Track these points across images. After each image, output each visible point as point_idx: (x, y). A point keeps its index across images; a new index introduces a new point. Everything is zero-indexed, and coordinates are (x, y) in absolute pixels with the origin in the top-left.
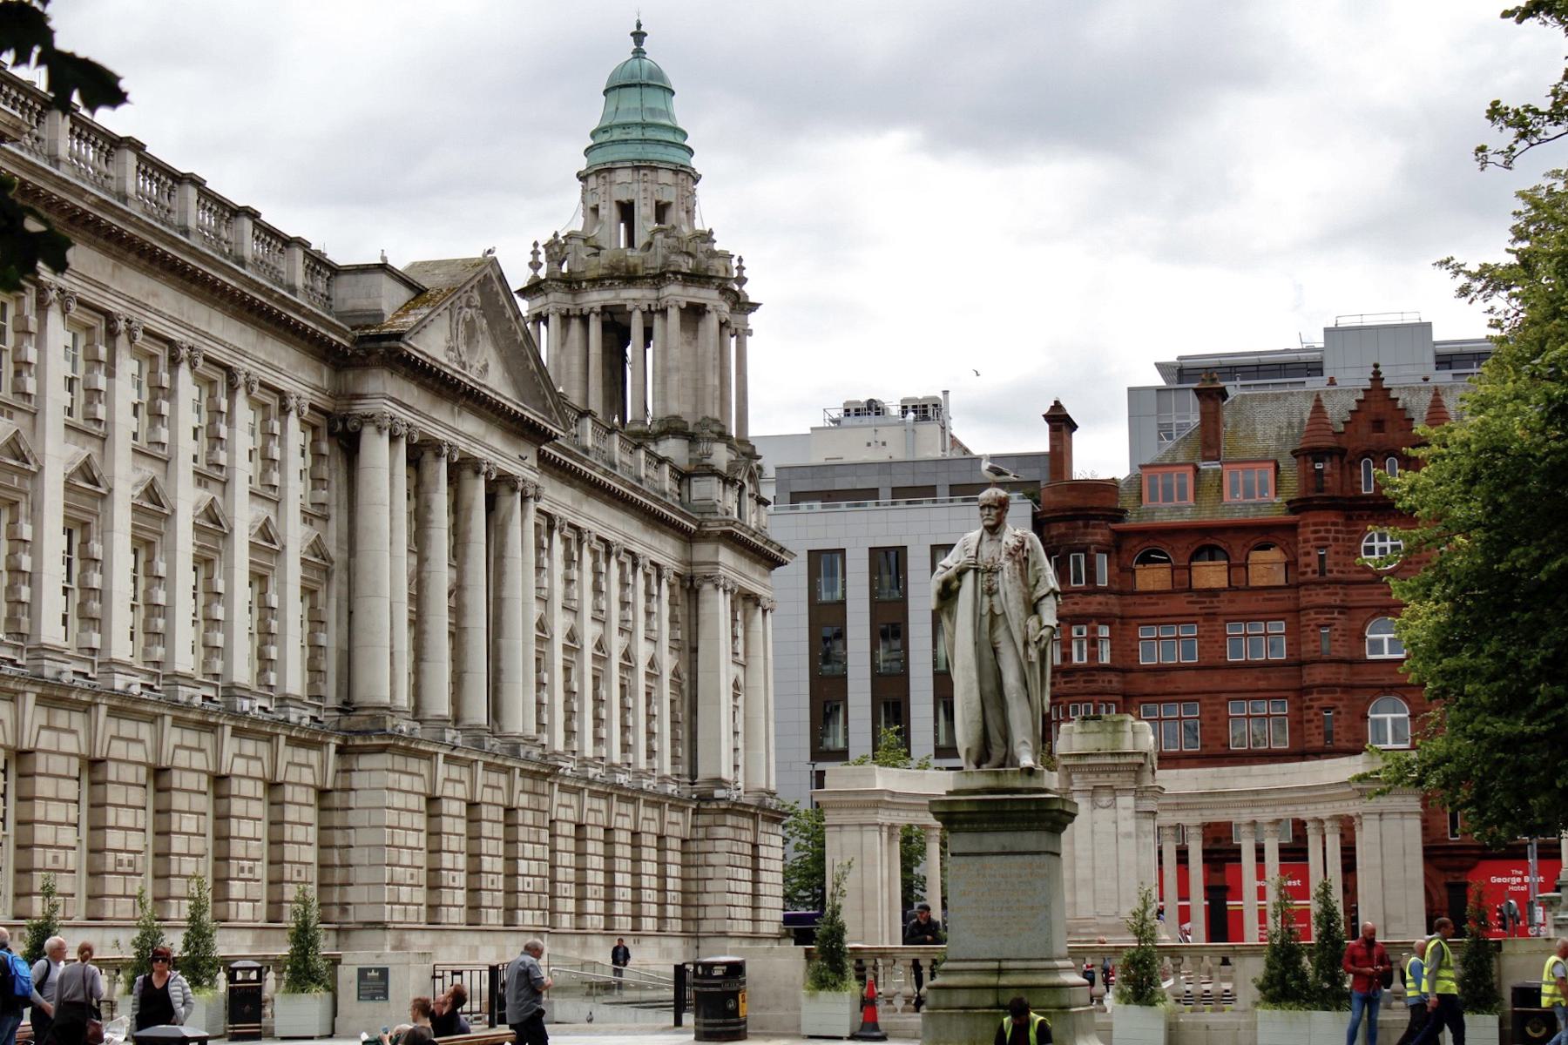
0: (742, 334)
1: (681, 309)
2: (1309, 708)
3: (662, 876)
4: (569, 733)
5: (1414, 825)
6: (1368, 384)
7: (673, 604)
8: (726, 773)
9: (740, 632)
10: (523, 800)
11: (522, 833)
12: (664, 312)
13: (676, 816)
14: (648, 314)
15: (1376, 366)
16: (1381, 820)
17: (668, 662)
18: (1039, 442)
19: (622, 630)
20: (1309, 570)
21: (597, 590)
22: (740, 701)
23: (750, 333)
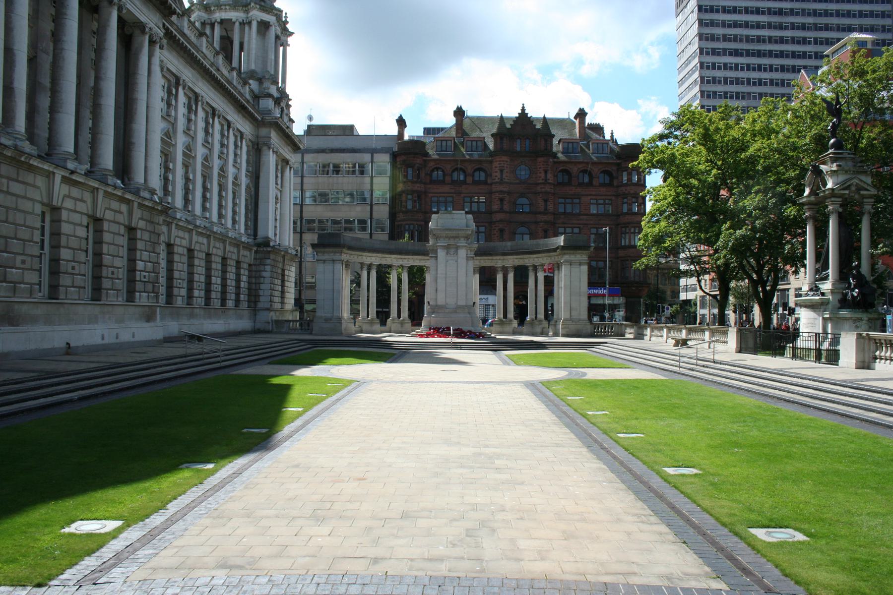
0: (285, 45)
1: (257, 21)
2: (494, 229)
3: (238, 281)
4: (186, 201)
5: (585, 268)
6: (520, 112)
7: (248, 152)
8: (271, 235)
9: (279, 175)
10: (142, 224)
11: (140, 245)
12: (250, 23)
13: (247, 253)
14: (242, 24)
15: (523, 104)
16: (571, 265)
17: (244, 181)
18: (394, 130)
19: (220, 157)
20: (497, 178)
21: (207, 132)
22: (278, 205)
23: (289, 45)
